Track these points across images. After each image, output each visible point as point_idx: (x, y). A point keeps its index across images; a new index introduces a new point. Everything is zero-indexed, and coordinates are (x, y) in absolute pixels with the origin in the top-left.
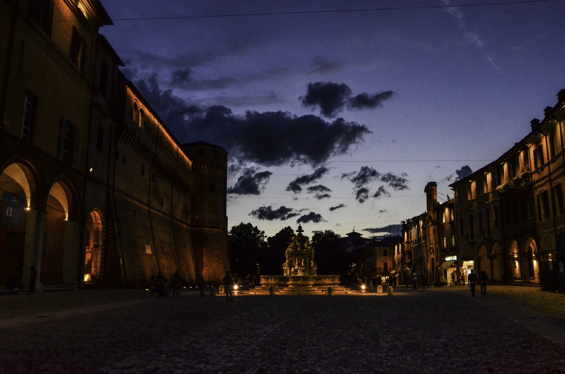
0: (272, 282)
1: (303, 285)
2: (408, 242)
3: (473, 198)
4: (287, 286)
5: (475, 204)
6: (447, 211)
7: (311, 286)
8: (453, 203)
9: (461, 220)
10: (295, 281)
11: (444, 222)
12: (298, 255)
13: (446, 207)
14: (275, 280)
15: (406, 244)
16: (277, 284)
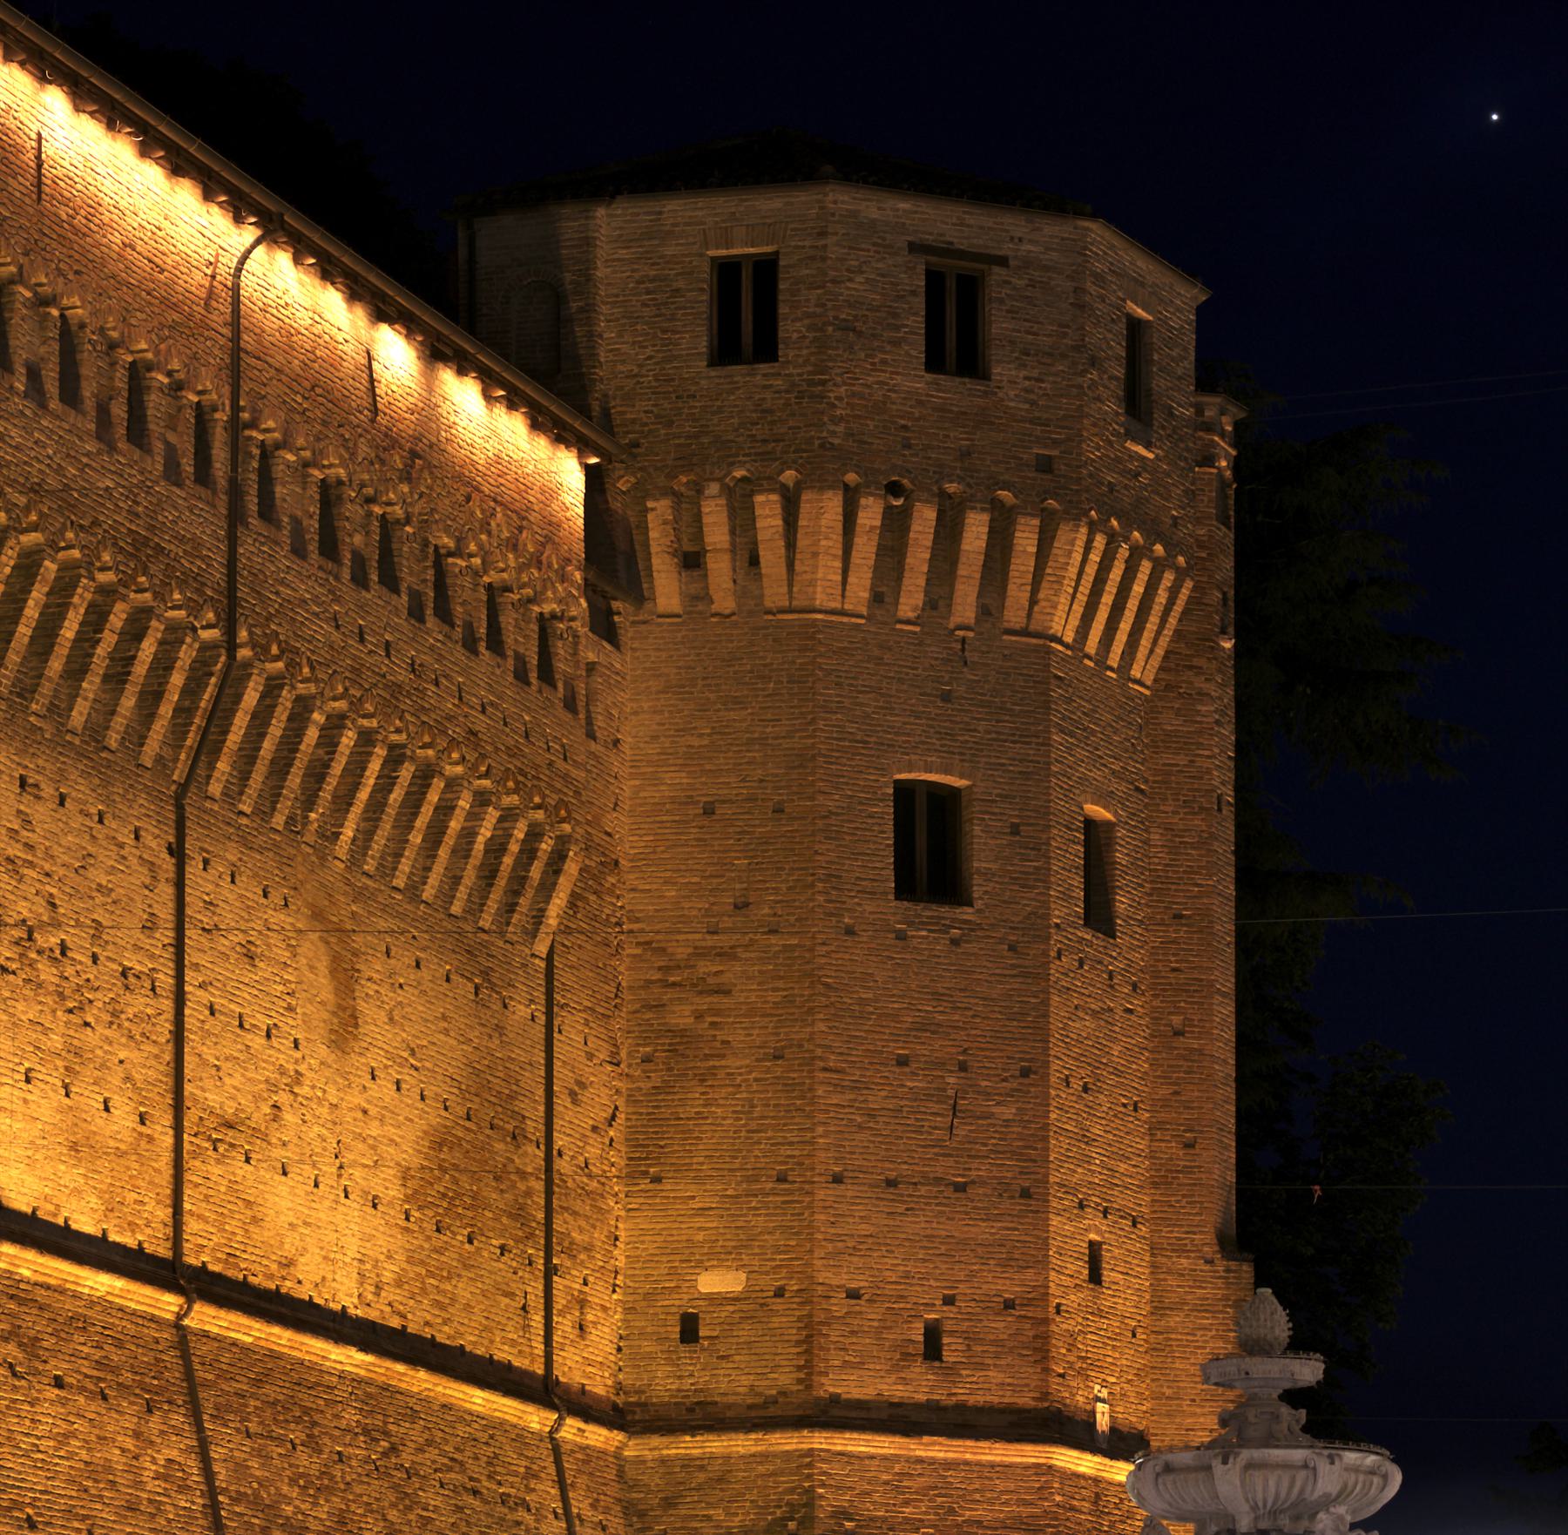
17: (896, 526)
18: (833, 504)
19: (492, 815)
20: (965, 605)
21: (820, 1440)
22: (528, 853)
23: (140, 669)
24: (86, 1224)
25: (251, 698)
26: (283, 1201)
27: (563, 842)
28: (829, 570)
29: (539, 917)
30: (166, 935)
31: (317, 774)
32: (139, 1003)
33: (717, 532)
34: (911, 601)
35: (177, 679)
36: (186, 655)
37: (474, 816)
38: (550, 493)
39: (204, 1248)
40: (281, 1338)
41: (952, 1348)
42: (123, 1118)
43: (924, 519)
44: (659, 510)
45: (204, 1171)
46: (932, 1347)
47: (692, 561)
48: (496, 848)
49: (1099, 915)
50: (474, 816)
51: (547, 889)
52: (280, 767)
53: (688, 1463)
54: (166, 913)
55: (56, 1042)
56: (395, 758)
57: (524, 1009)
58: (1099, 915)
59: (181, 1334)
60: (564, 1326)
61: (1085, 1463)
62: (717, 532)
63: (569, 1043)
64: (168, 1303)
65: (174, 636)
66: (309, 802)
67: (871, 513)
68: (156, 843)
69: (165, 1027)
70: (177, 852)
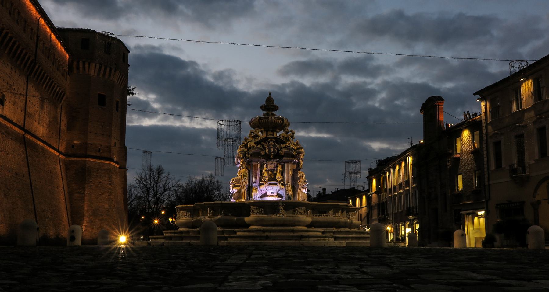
0: (207, 218)
1: (284, 224)
2: (378, 191)
3: (524, 107)
4: (247, 225)
5: (527, 115)
6: (466, 134)
7: (305, 228)
8: (481, 121)
9: (497, 144)
10: (266, 213)
11: (459, 151)
12: (267, 157)
13: (466, 128)
14: (214, 214)
15: (374, 196)
16: (219, 223)
17: (100, 68)
18: (94, 65)
19: (58, 89)
20: (107, 77)
21: (87, 159)
22: (61, 94)
23: (26, 59)
24: (14, 121)
25: (37, 66)
26: (36, 124)
27: (64, 94)
28: (93, 71)
29: (61, 102)
30: (25, 91)
31: (42, 78)
32: (22, 98)
33: (81, 66)
34: (101, 75)
35: (29, 62)
36: (31, 59)
37: (57, 88)
38: (66, 57)
39: (27, 128)
40: (34, 140)
41: (101, 151)
42: (19, 111)
43: (103, 68)
44: (75, 63)
45: (27, 119)
46: (99, 151)
47: (78, 68)
48: (58, 92)
49: (117, 110)
50: (57, 88)
51: (62, 98)
52: (38, 76)
53: (72, 161)
54: (25, 88)
55: (13, 99)
56: (50, 79)
57: (59, 110)
58: (117, 110)
59: (24, 137)
60: (60, 145)
61: (114, 164)
62: (81, 66)
63: (63, 115)
64: (23, 133)
65: (30, 57)
66: (41, 81)
67: (98, 66)
68: (25, 80)
69: (24, 102)
70: (27, 82)
